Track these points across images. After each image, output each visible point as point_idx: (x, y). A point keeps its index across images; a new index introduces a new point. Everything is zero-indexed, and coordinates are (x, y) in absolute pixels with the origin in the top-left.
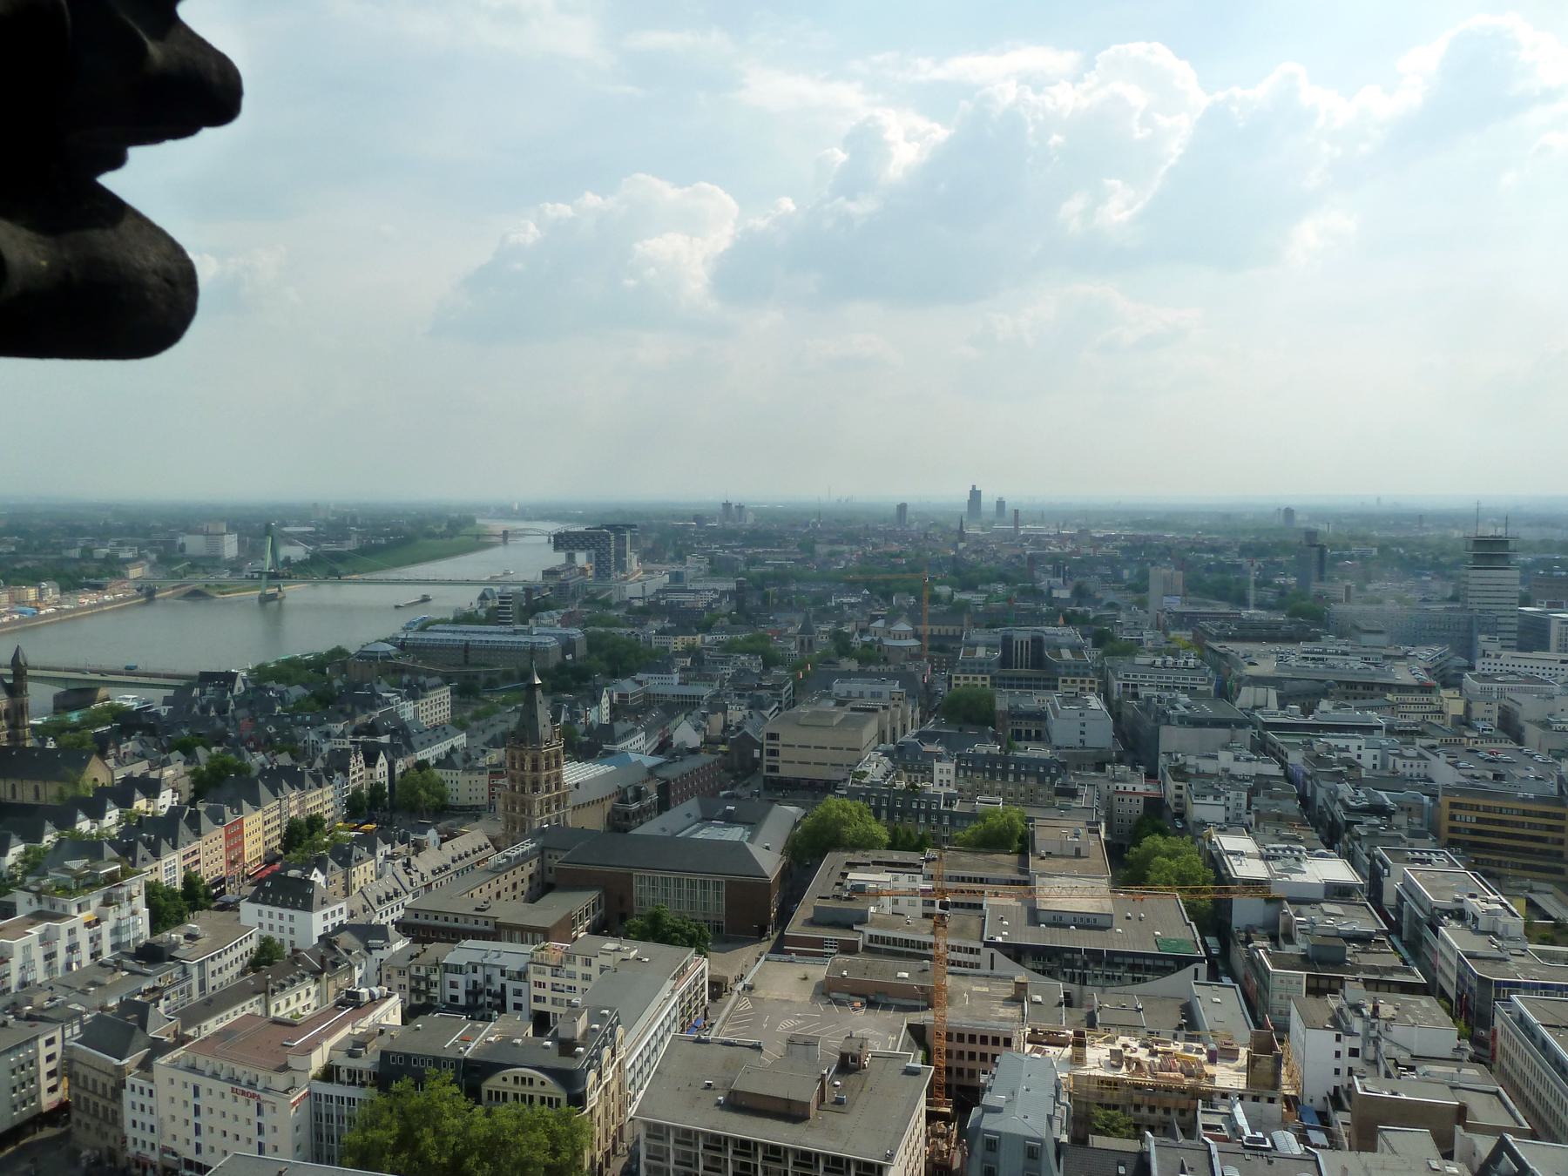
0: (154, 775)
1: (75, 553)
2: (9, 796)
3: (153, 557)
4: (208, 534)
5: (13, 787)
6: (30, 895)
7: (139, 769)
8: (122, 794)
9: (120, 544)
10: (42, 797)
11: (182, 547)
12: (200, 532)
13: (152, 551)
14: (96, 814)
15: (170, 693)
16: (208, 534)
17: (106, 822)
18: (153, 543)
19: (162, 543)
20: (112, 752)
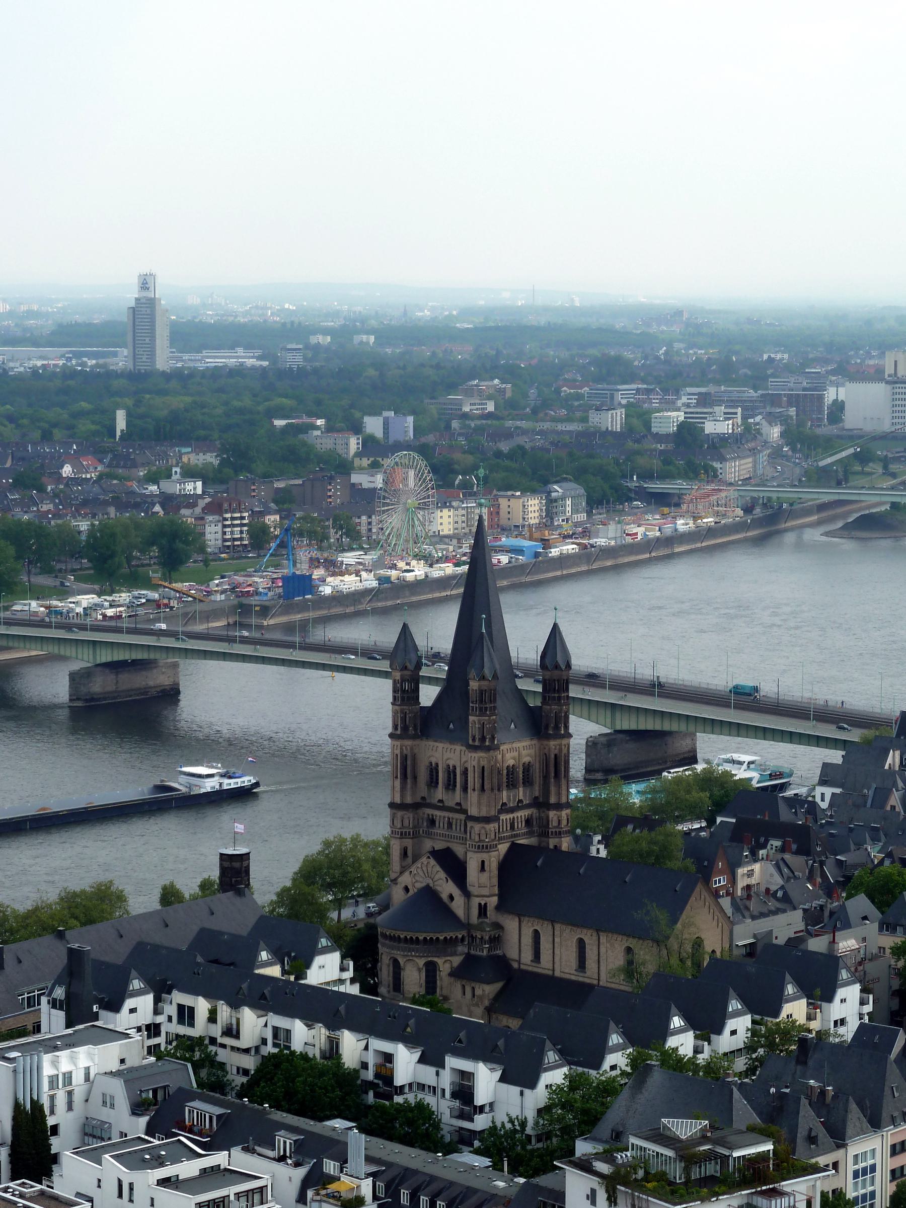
0: (817, 945)
1: (613, 420)
2: (527, 956)
3: (775, 432)
4: (895, 381)
5: (536, 935)
6: (593, 1182)
7: (785, 926)
8: (760, 976)
9: (705, 400)
10: (591, 964)
11: (838, 407)
12: (877, 375)
13: (771, 419)
14: (707, 1025)
15: (836, 756)
16: (895, 381)
17: (725, 1042)
18: (774, 400)
19: (793, 400)
20: (720, 881)
